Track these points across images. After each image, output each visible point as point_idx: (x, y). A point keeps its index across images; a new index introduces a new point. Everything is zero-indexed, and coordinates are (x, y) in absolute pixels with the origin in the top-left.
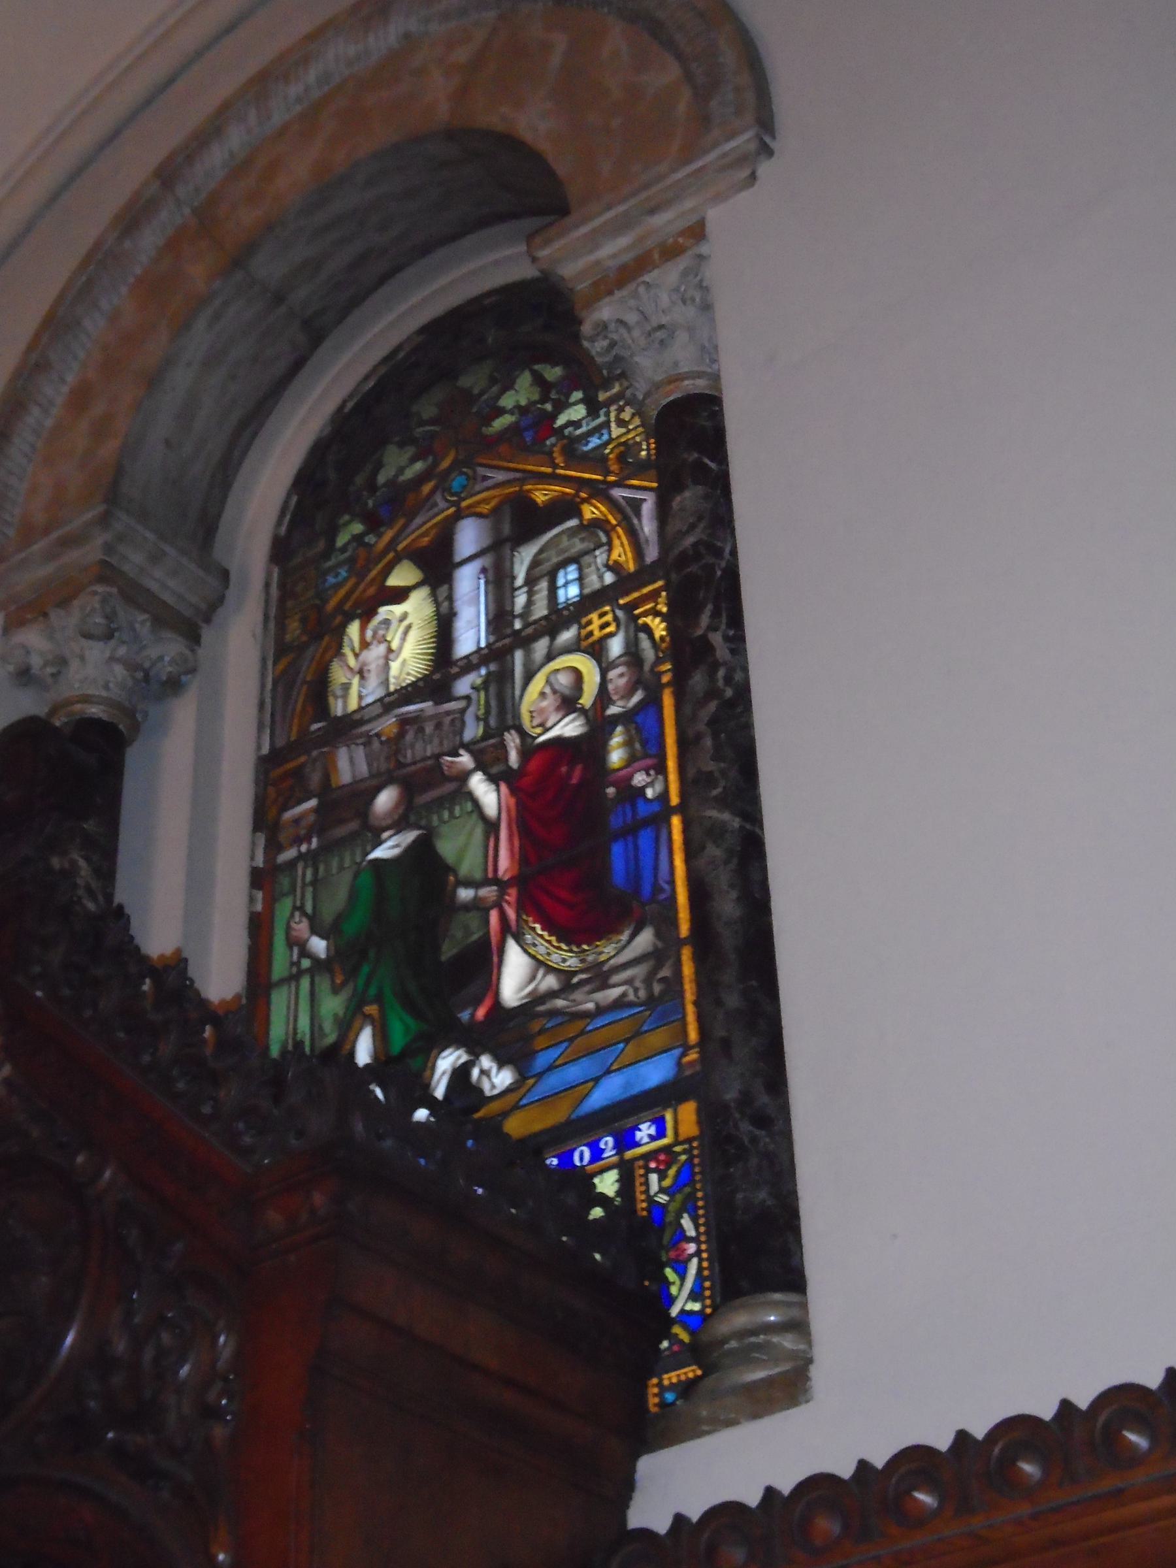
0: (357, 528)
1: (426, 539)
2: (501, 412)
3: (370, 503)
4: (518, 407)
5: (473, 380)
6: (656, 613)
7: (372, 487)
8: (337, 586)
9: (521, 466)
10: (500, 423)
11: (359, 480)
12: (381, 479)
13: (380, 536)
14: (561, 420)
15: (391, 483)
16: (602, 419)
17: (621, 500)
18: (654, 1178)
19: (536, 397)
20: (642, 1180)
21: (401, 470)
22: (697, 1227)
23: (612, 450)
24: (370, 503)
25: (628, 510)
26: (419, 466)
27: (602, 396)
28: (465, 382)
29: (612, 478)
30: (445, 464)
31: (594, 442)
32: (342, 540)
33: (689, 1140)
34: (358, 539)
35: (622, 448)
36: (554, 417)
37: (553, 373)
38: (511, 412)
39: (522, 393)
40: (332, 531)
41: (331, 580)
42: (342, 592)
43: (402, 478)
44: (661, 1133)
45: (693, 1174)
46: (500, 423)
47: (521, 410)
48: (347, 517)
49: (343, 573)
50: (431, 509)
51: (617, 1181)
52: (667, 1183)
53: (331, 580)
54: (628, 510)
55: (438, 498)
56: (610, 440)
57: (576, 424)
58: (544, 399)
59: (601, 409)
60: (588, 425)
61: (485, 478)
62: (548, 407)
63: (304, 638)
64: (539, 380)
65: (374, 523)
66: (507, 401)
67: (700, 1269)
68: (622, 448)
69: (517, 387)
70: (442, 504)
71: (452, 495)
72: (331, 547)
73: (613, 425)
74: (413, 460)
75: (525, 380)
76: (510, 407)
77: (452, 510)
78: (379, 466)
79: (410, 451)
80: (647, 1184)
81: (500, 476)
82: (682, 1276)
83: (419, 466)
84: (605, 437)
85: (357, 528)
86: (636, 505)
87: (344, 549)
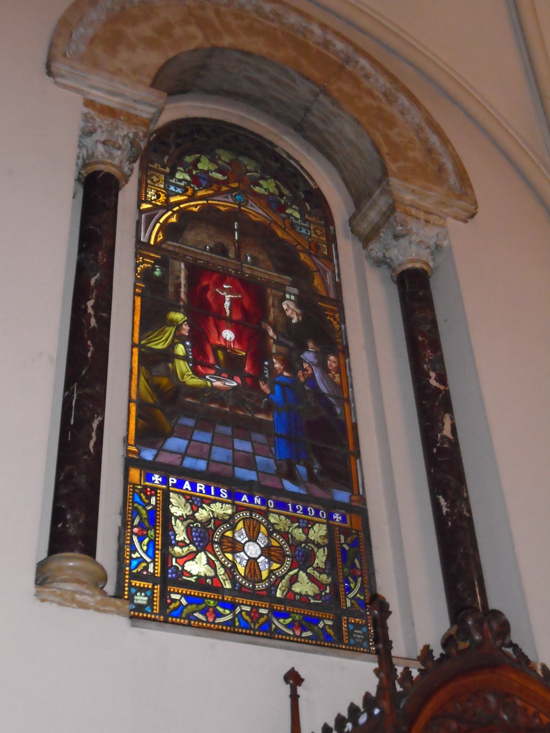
2: (260, 186)
8: (177, 194)
10: (257, 189)
11: (188, 159)
13: (200, 190)
14: (289, 211)
26: (219, 176)
32: (179, 176)
38: (266, 190)
46: (257, 189)
48: (181, 169)
50: (225, 198)
53: (172, 188)
57: (297, 219)
64: (277, 186)
74: (217, 171)
78: (198, 161)
79: (216, 167)
83: (219, 176)
87: (180, 181)
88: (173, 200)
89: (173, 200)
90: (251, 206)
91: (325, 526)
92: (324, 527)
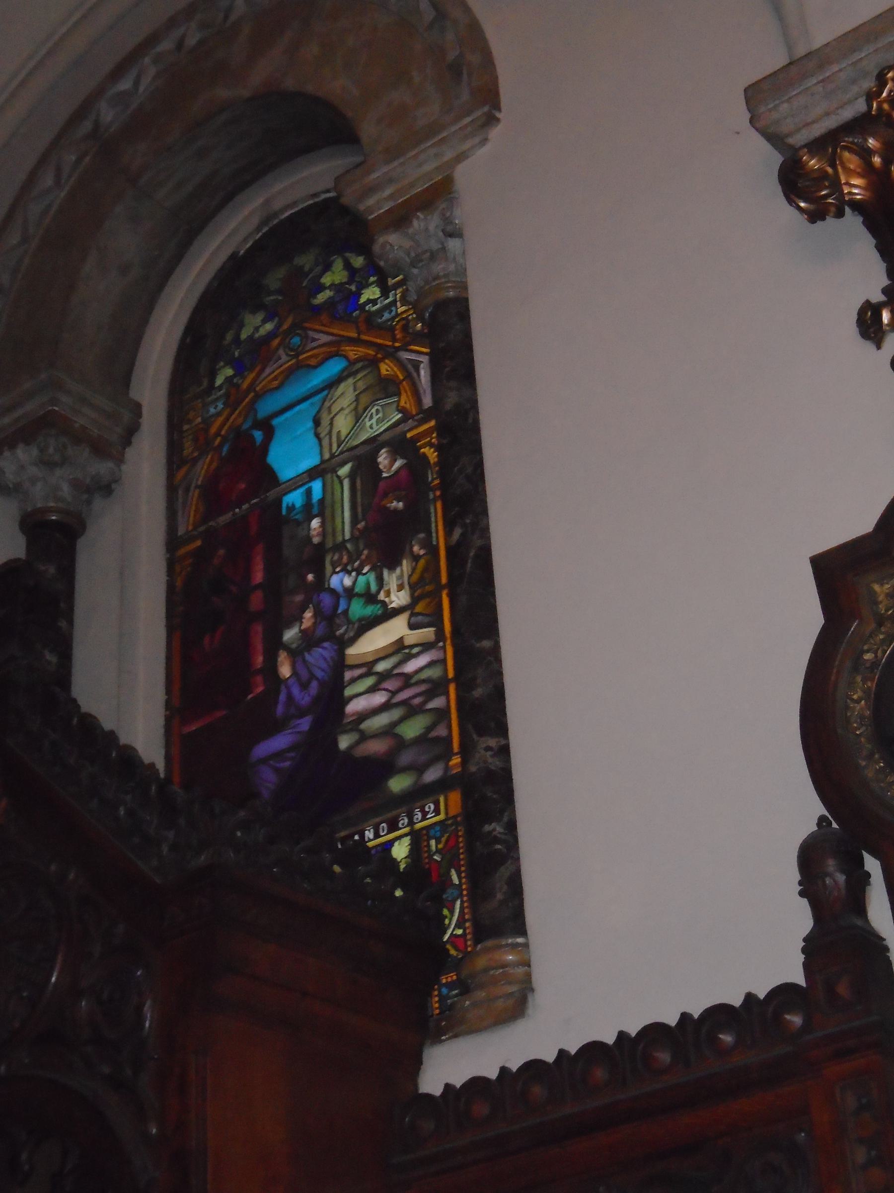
0: (229, 372)
1: (277, 382)
3: (237, 354)
4: (332, 286)
5: (305, 260)
6: (431, 445)
7: (237, 340)
9: (335, 331)
10: (322, 297)
11: (229, 337)
12: (244, 336)
14: (363, 299)
15: (250, 338)
16: (391, 299)
17: (406, 361)
18: (433, 843)
19: (345, 280)
20: (425, 844)
21: (257, 329)
22: (460, 878)
23: (398, 322)
24: (237, 354)
25: (410, 367)
26: (269, 327)
27: (391, 282)
28: (299, 261)
29: (397, 345)
30: (285, 327)
31: (387, 316)
32: (219, 381)
33: (455, 817)
34: (229, 380)
35: (404, 322)
36: (358, 295)
37: (358, 261)
39: (336, 275)
40: (213, 375)
41: (212, 410)
42: (221, 419)
43: (257, 335)
44: (437, 812)
45: (457, 842)
46: (322, 297)
47: (337, 288)
48: (222, 364)
49: (220, 406)
51: (409, 845)
52: (440, 846)
53: (212, 410)
54: (410, 367)
55: (281, 352)
56: (397, 315)
57: (374, 302)
58: (351, 281)
59: (391, 292)
60: (381, 303)
61: (314, 340)
62: (353, 288)
63: (196, 454)
64: (348, 266)
65: (240, 368)
66: (327, 280)
67: (462, 908)
68: (404, 322)
69: (333, 269)
70: (284, 358)
71: (292, 350)
72: (211, 387)
73: (398, 304)
74: (264, 321)
75: (338, 264)
76: (328, 284)
77: (293, 361)
78: (241, 325)
80: (428, 846)
81: (324, 338)
82: (452, 912)
83: (269, 327)
84: (393, 313)
85: (229, 372)
86: (416, 365)
87: (220, 388)
88: (213, 430)
89: (213, 430)
90: (314, 340)
91: (409, 838)
92: (407, 841)
